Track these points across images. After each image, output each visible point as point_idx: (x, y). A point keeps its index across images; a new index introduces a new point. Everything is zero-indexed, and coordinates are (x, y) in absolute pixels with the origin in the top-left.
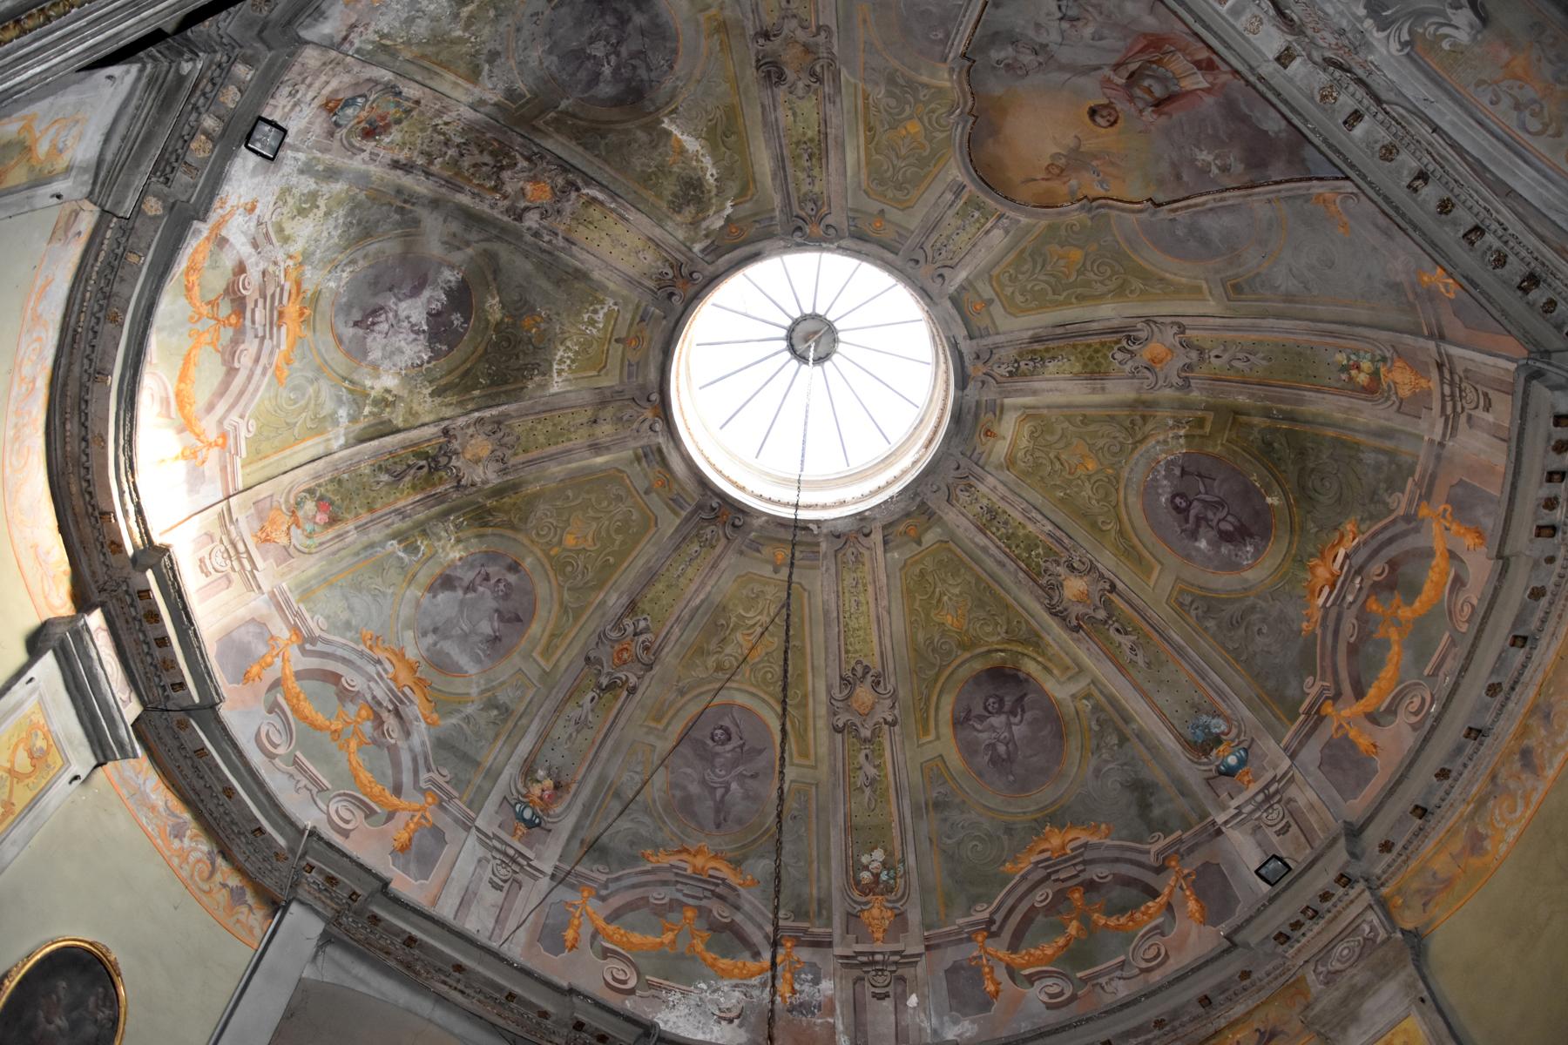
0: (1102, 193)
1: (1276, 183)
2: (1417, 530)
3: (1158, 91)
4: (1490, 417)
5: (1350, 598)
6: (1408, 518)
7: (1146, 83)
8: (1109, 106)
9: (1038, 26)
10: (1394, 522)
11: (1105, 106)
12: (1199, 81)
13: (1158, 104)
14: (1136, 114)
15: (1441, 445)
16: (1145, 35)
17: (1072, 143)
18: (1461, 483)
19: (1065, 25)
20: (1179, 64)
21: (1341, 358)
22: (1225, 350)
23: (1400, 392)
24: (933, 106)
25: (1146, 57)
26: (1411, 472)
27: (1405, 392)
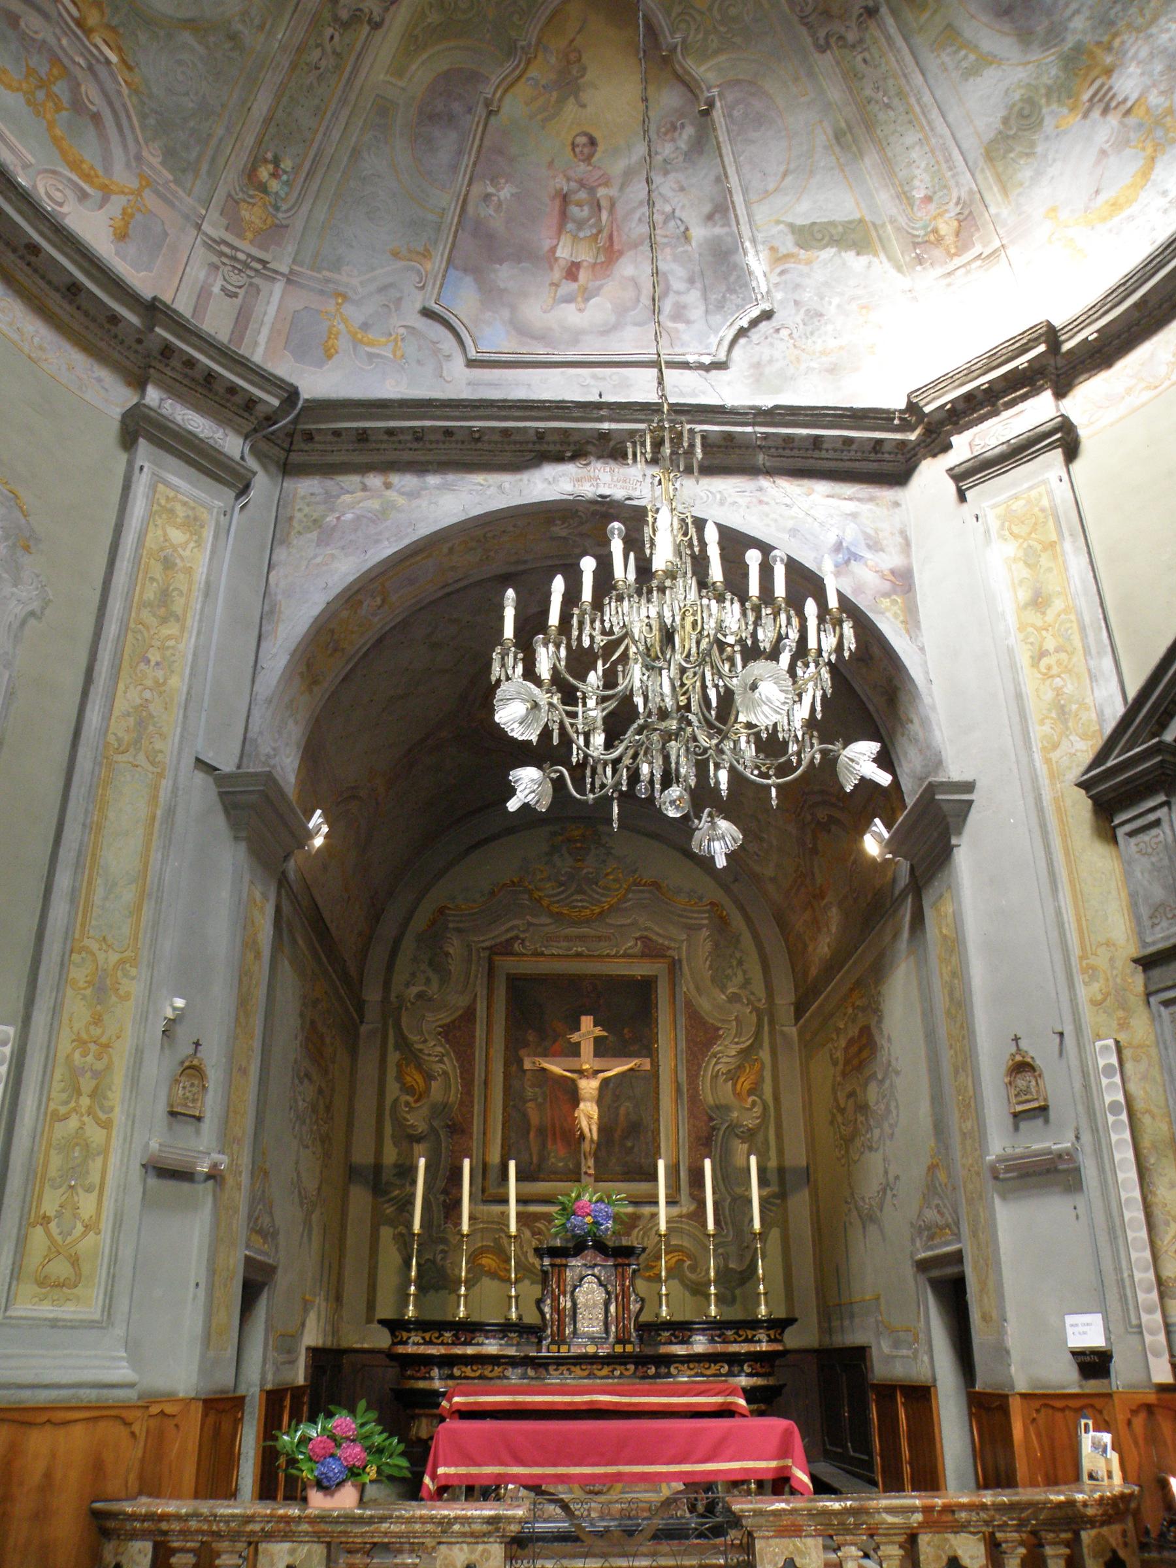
0: (529, 74)
1: (456, 232)
2: (128, 165)
3: (574, 210)
4: (216, 289)
5: (64, 42)
6: (139, 158)
7: (586, 208)
8: (588, 159)
9: (682, 189)
10: (137, 141)
11: (591, 156)
12: (564, 252)
13: (565, 199)
14: (571, 173)
15: (199, 227)
16: (621, 253)
17: (585, 96)
18: (166, 234)
19: (668, 209)
20: (585, 255)
21: (287, 164)
22: (334, 52)
23: (243, 205)
24: (700, 36)
25: (605, 234)
26: (177, 181)
27: (245, 214)
